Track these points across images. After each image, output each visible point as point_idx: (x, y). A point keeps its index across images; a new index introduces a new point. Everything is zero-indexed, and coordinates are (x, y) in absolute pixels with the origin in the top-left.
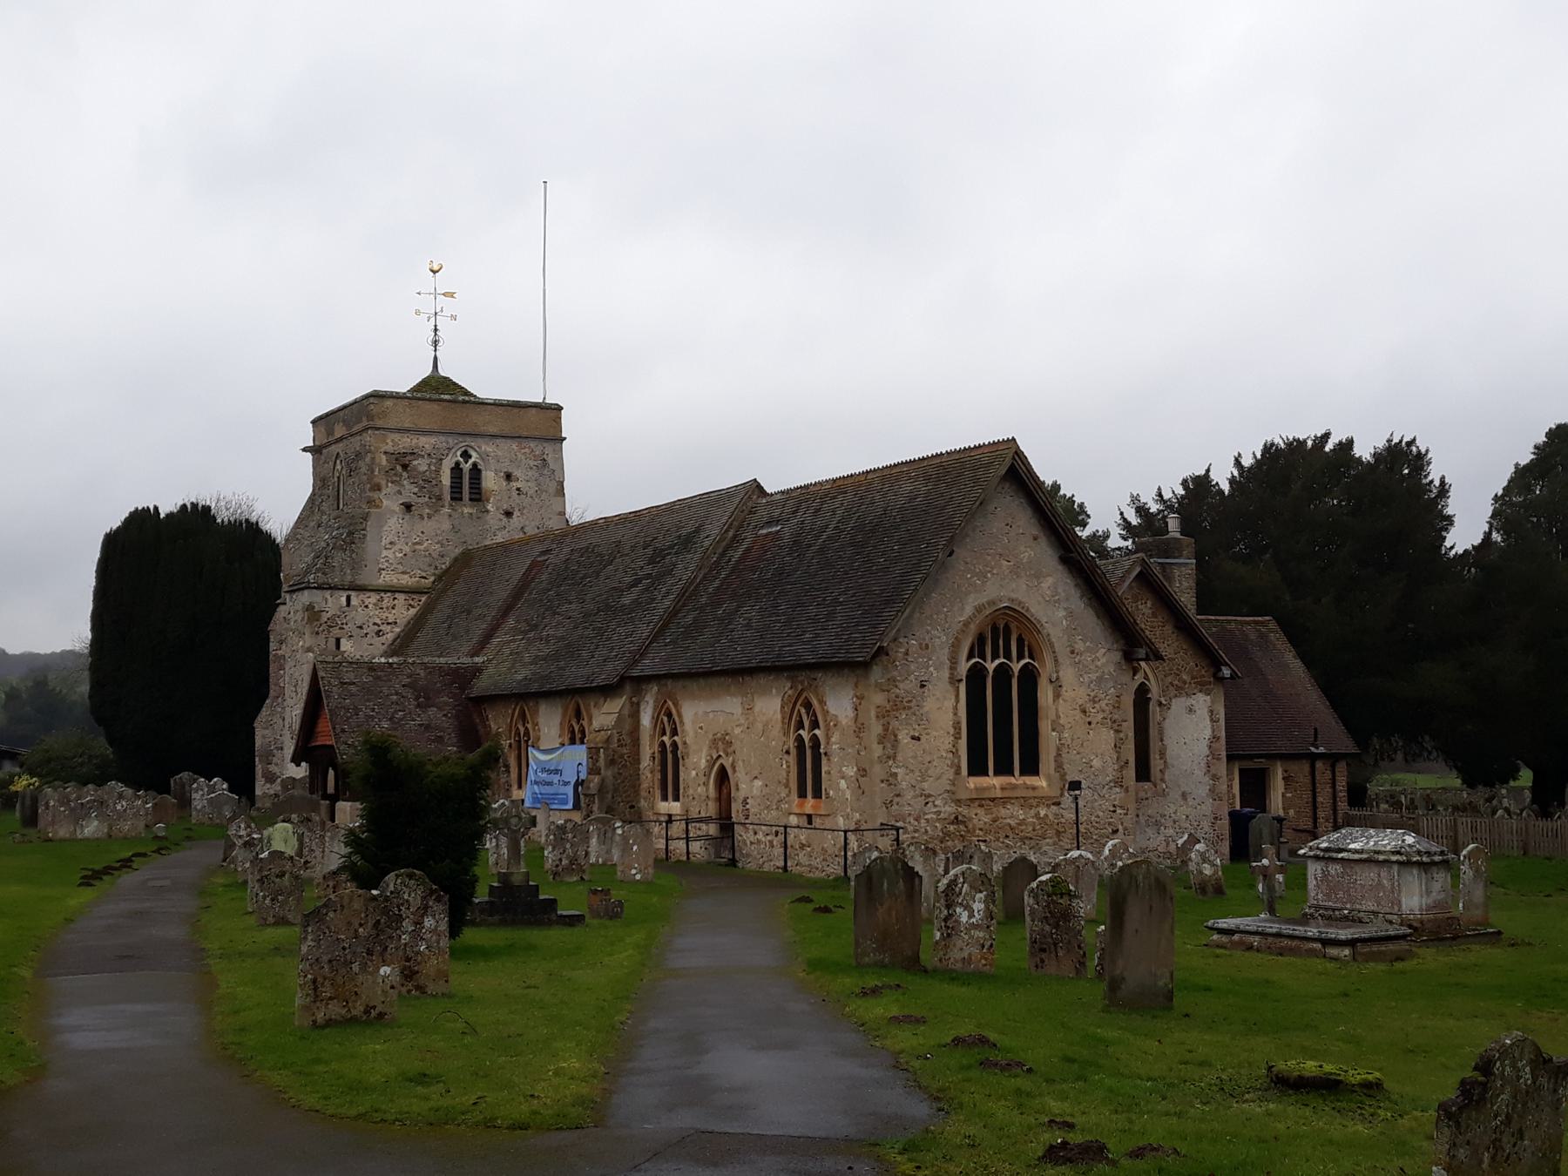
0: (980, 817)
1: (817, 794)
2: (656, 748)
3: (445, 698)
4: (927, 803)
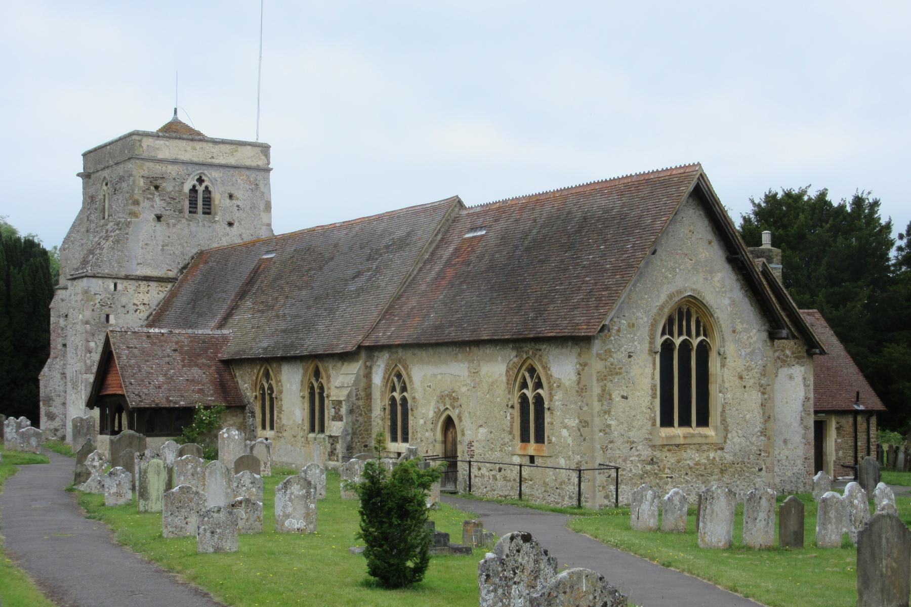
0: (669, 459)
1: (540, 439)
2: (387, 402)
3: (204, 361)
4: (631, 448)
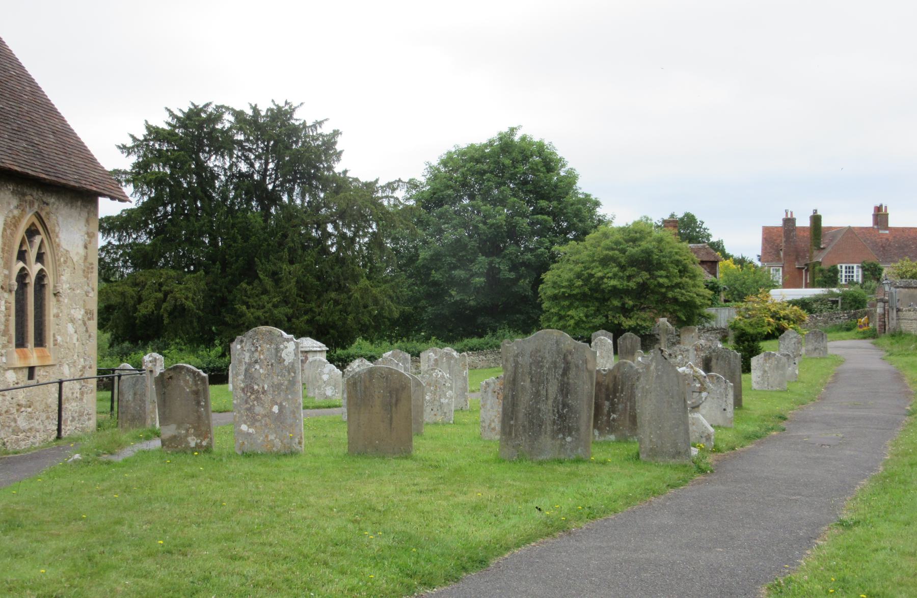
1: (40, 341)
